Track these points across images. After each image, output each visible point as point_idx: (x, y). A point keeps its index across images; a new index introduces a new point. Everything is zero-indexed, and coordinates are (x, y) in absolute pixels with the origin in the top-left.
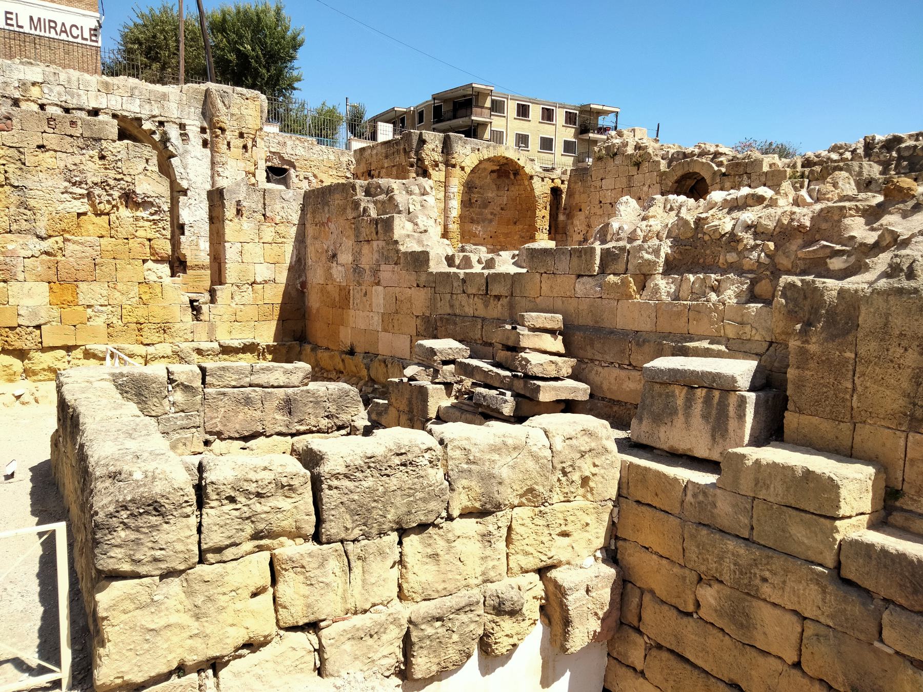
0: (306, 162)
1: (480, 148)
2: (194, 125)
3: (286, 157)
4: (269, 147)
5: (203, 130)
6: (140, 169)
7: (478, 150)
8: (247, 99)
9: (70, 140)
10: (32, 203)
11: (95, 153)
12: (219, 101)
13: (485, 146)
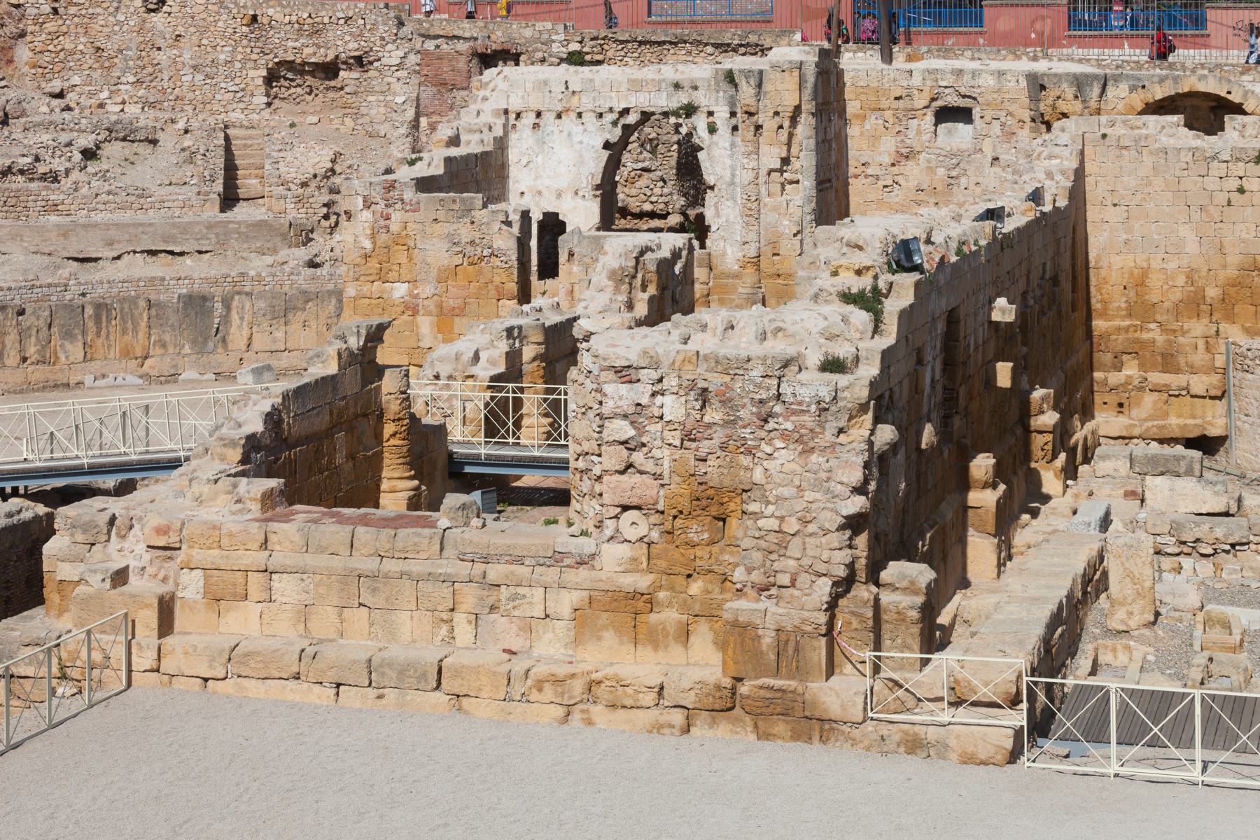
0: (996, 96)
1: (1146, 84)
2: (722, 113)
3: (963, 90)
4: (937, 81)
5: (733, 114)
6: (497, 228)
7: (1144, 87)
8: (783, 71)
9: (452, 213)
10: (429, 260)
11: (468, 220)
12: (744, 82)
13: (1156, 79)
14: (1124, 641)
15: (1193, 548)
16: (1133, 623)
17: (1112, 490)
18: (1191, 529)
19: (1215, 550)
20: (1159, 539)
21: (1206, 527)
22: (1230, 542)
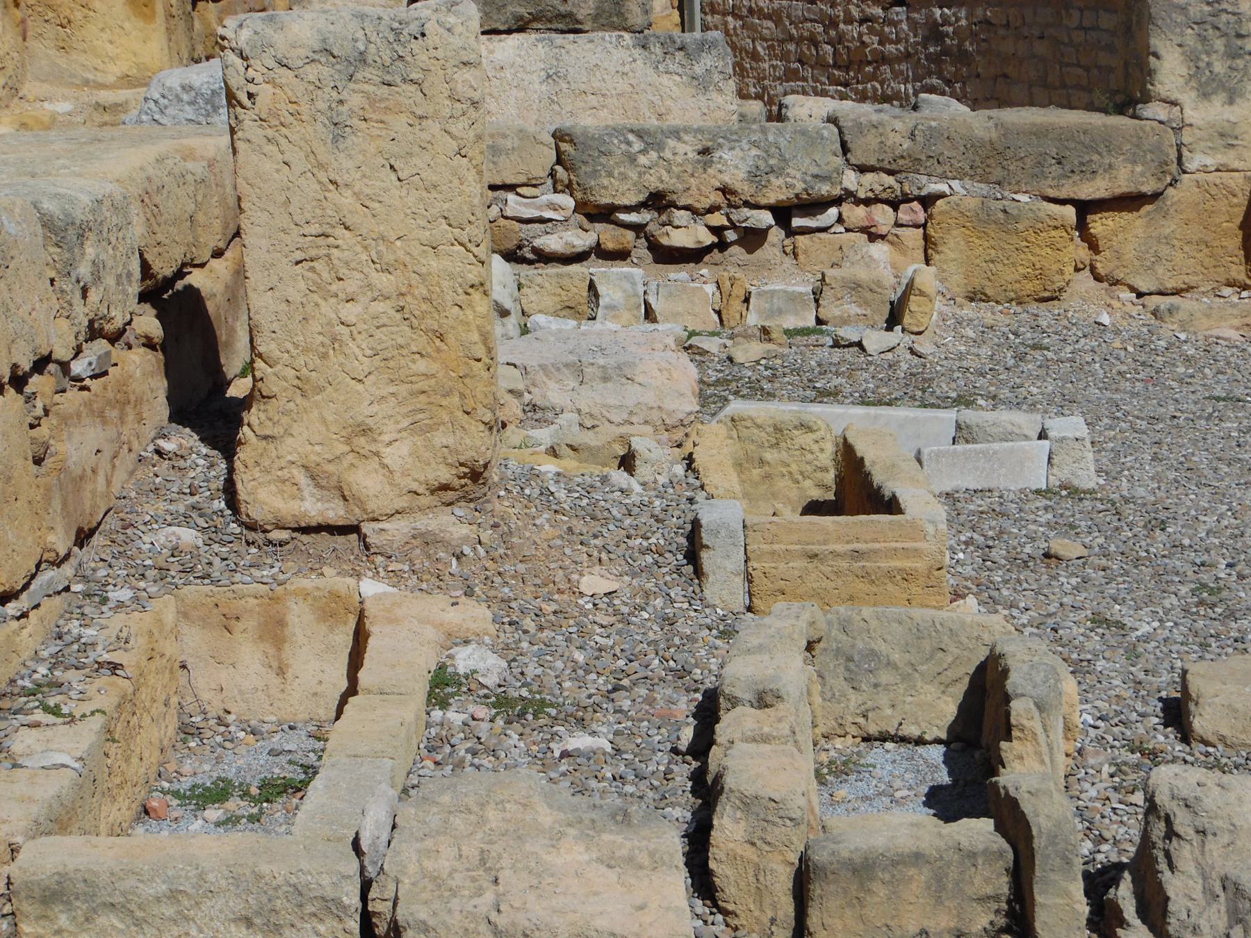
14: (333, 579)
15: (638, 228)
18: (632, 159)
19: (717, 231)
20: (514, 204)
22: (772, 197)
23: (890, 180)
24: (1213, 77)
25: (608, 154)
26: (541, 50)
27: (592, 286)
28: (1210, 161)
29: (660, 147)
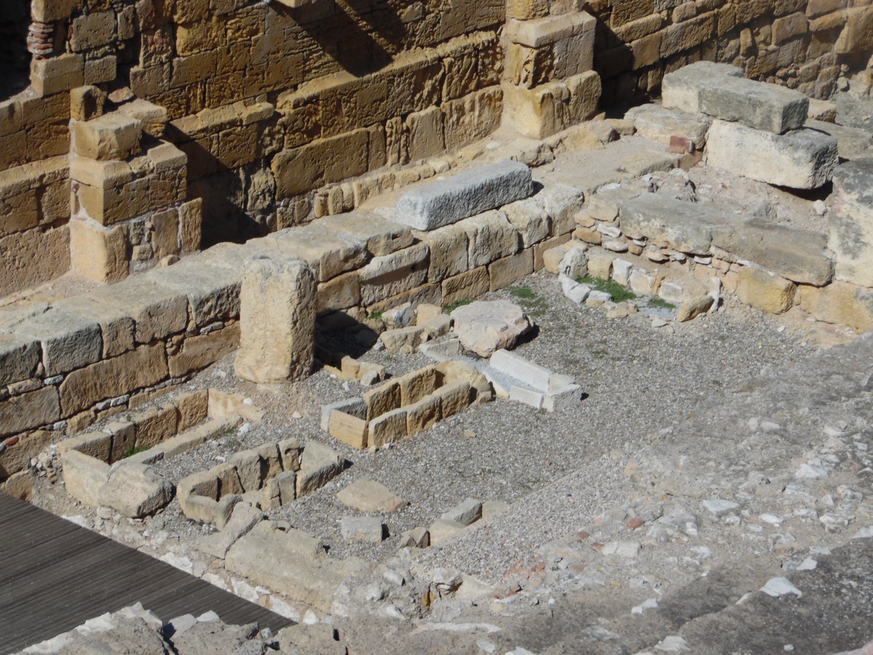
16: (261, 375)
17: (661, 132)
18: (639, 223)
21: (657, 223)
23: (726, 254)
24: (848, 248)
25: (632, 218)
26: (737, 133)
27: (611, 266)
28: (845, 278)
29: (649, 221)
